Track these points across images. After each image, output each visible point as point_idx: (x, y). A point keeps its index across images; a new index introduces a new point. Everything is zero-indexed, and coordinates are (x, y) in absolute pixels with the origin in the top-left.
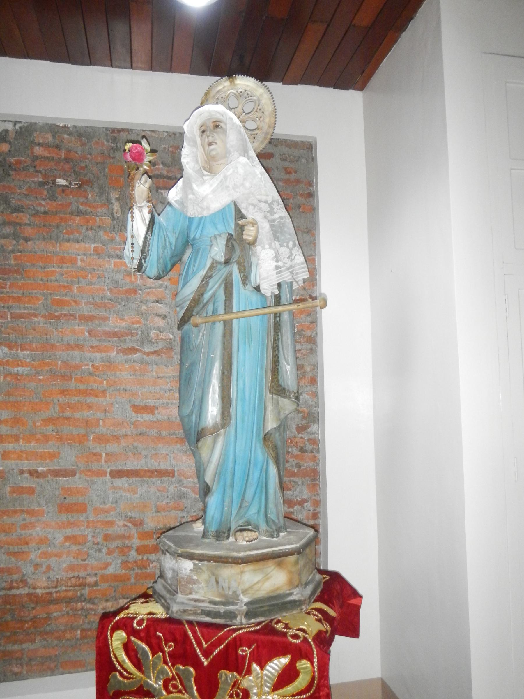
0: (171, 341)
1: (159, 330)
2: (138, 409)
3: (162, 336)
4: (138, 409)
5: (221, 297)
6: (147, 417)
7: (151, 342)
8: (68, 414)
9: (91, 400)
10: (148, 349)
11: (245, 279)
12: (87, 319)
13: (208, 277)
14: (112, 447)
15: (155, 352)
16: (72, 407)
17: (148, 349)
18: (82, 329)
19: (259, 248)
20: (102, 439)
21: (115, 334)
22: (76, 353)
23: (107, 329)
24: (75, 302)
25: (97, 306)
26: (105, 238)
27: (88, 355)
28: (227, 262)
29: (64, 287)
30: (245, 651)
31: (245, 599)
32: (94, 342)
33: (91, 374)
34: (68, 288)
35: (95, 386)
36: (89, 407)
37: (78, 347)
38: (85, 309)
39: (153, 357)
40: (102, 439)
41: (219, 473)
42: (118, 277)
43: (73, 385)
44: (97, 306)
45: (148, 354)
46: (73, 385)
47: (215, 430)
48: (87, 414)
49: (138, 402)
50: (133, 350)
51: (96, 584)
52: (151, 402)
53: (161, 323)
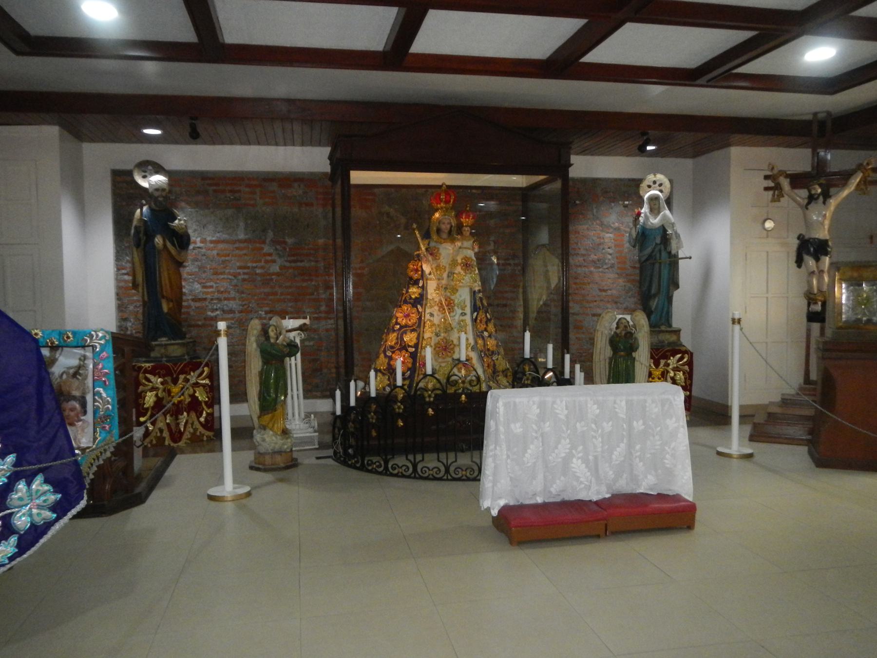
0: (613, 264)
1: (609, 260)
2: (601, 290)
3: (610, 262)
4: (601, 290)
5: (658, 255)
6: (604, 294)
7: (606, 264)
8: (577, 292)
9: (584, 286)
10: (605, 267)
11: (665, 249)
12: (583, 255)
13: (655, 248)
14: (591, 305)
15: (607, 268)
16: (577, 289)
17: (605, 267)
18: (581, 259)
19: (672, 241)
20: (588, 302)
21: (593, 261)
22: (579, 269)
23: (590, 259)
24: (579, 249)
25: (587, 250)
26: (590, 223)
27: (583, 269)
28: (660, 244)
29: (575, 243)
30: (669, 354)
31: (666, 342)
32: (586, 264)
33: (585, 277)
34: (577, 244)
35: (586, 281)
36: (584, 289)
37: (580, 266)
38: (583, 252)
39: (607, 270)
40: (588, 302)
41: (656, 309)
42: (595, 238)
43: (578, 281)
44: (587, 250)
45: (604, 269)
46: (578, 281)
47: (655, 296)
48: (583, 292)
49: (601, 288)
50: (599, 268)
51: (585, 356)
52: (605, 288)
53: (610, 257)
